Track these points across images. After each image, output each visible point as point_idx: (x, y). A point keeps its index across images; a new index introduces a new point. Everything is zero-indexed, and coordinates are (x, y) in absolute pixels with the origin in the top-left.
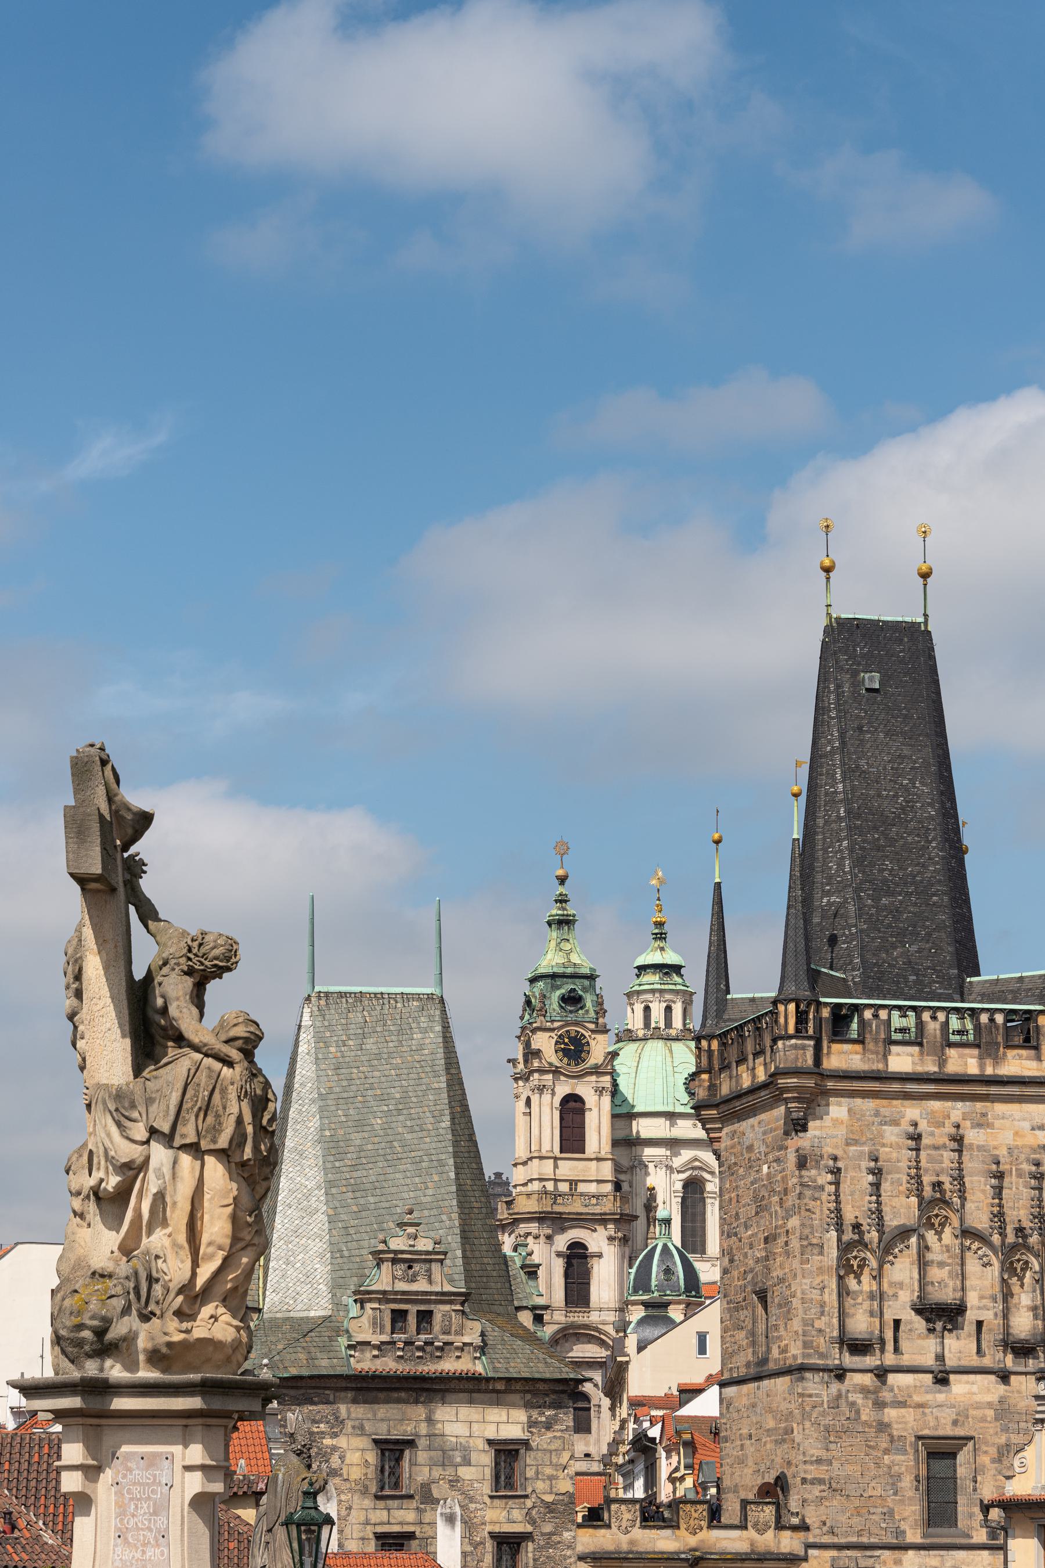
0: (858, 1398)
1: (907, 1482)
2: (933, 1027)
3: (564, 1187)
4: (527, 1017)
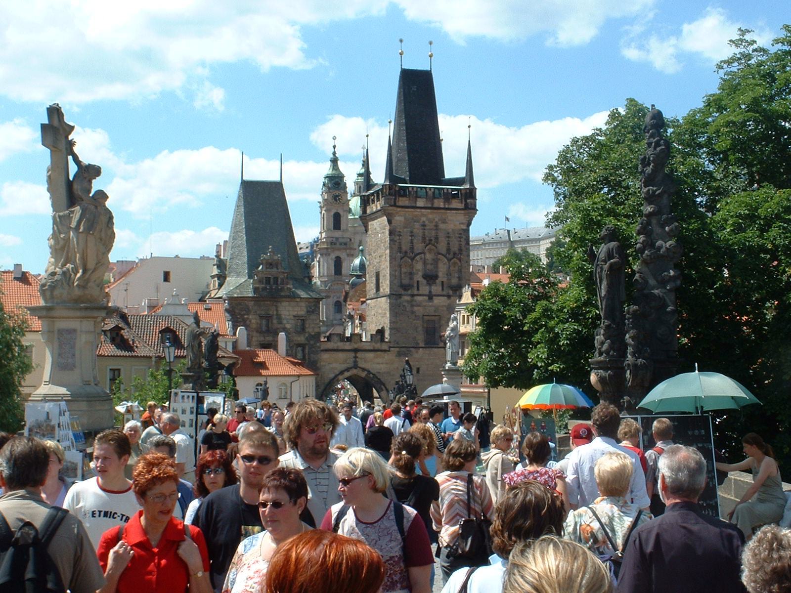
0: (406, 304)
1: (420, 329)
2: (430, 193)
3: (334, 239)
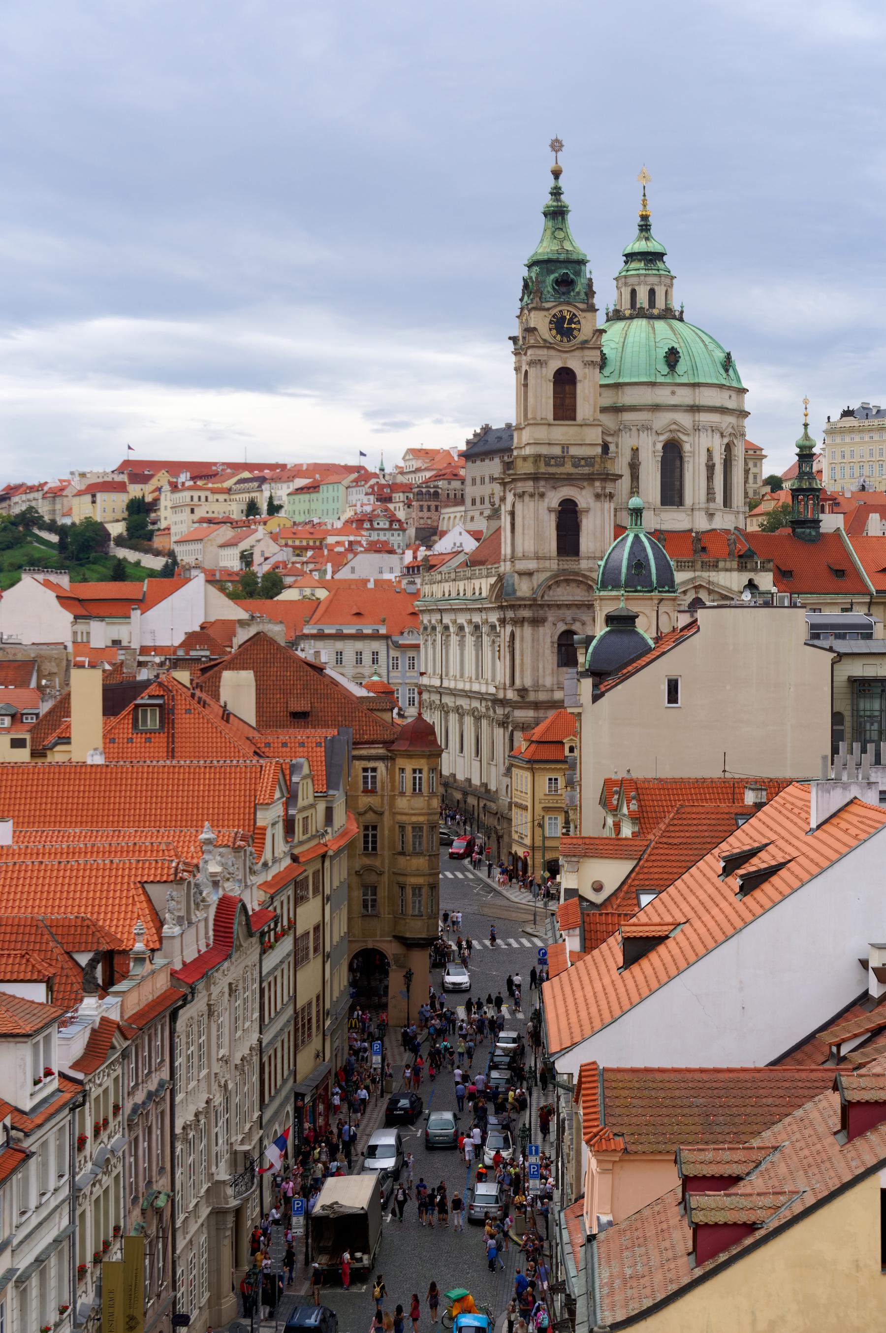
4: (526, 298)
